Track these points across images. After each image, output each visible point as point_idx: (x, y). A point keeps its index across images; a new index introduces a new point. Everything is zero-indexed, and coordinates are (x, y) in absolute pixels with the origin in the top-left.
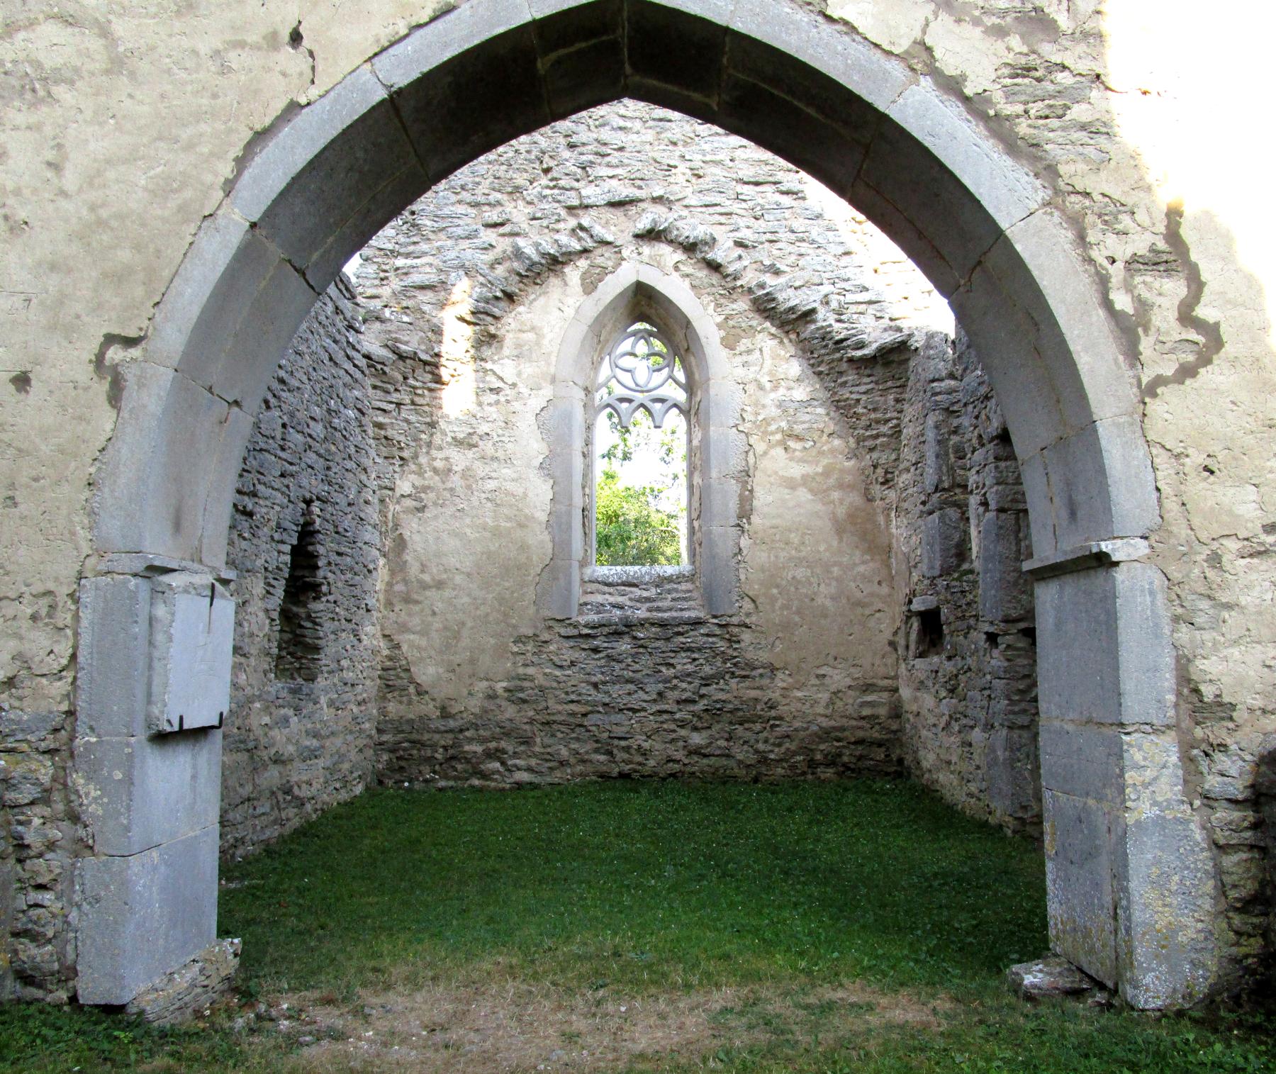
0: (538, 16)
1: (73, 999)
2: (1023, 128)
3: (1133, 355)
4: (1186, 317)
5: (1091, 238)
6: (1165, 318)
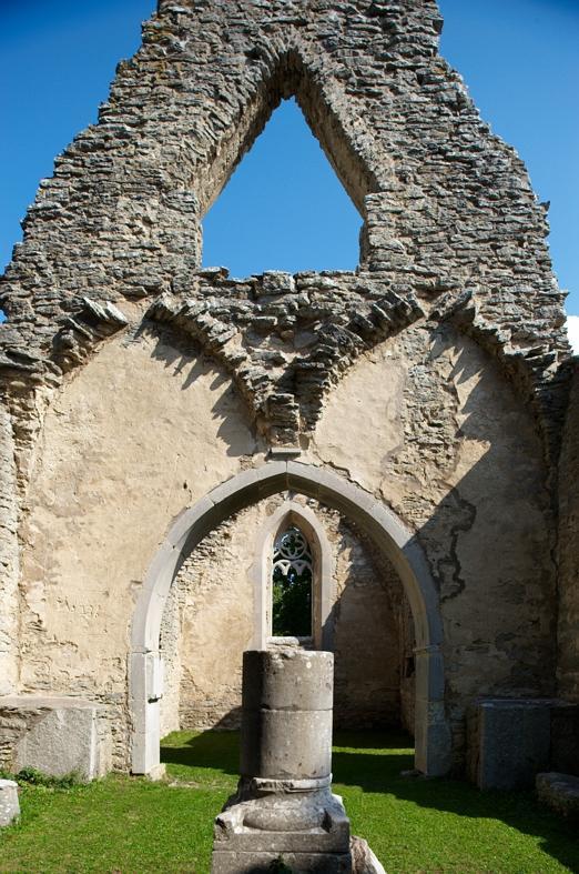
0: (261, 479)
1: (131, 772)
2: (410, 518)
3: (439, 589)
4: (455, 578)
5: (429, 553)
6: (449, 579)
